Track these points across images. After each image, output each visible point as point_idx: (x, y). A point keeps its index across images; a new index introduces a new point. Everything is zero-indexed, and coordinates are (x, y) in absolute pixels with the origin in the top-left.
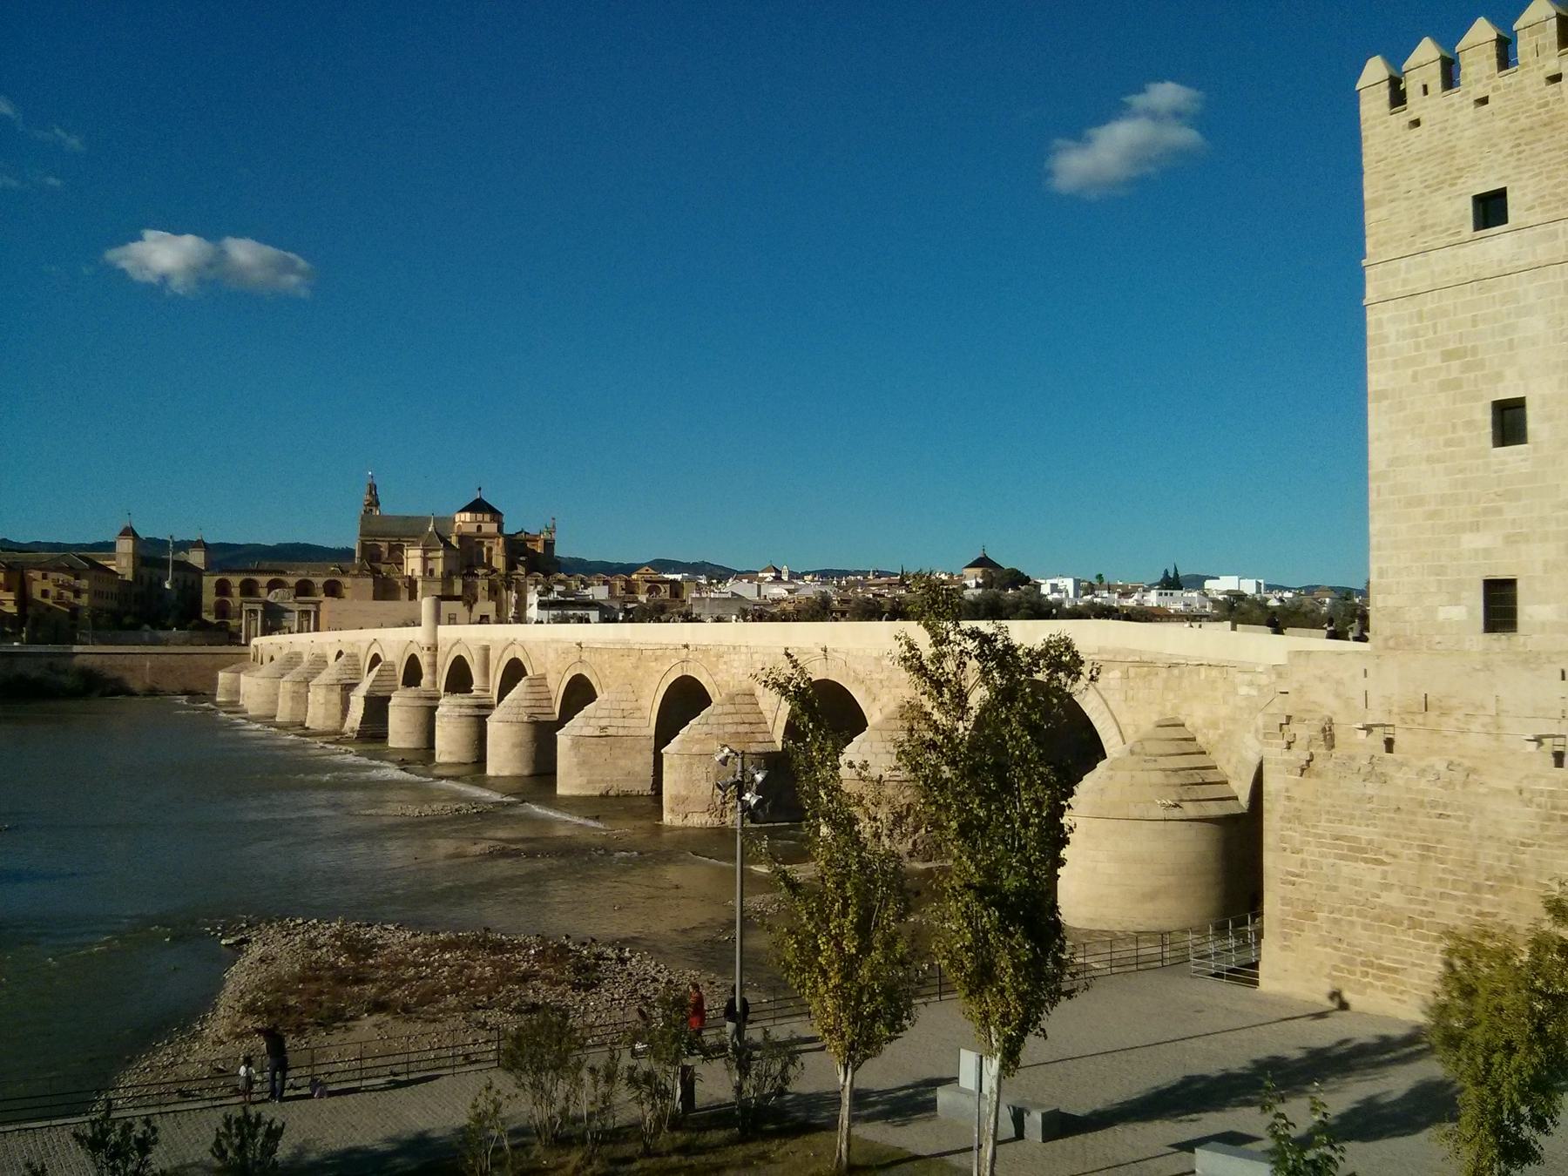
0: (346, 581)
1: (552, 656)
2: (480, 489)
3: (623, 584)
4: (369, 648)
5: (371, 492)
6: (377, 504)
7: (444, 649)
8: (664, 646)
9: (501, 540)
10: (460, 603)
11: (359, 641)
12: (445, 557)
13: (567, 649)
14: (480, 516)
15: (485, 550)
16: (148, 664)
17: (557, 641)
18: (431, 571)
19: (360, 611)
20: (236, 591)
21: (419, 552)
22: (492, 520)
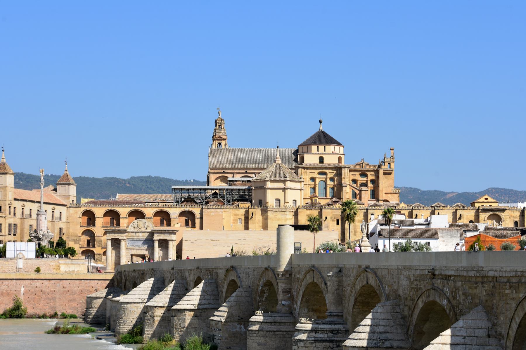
1: (405, 283)
4: (226, 275)
7: (298, 276)
8: (519, 273)
11: (217, 268)
13: (420, 276)
14: (321, 148)
16: (23, 289)
17: (410, 268)
19: (212, 240)
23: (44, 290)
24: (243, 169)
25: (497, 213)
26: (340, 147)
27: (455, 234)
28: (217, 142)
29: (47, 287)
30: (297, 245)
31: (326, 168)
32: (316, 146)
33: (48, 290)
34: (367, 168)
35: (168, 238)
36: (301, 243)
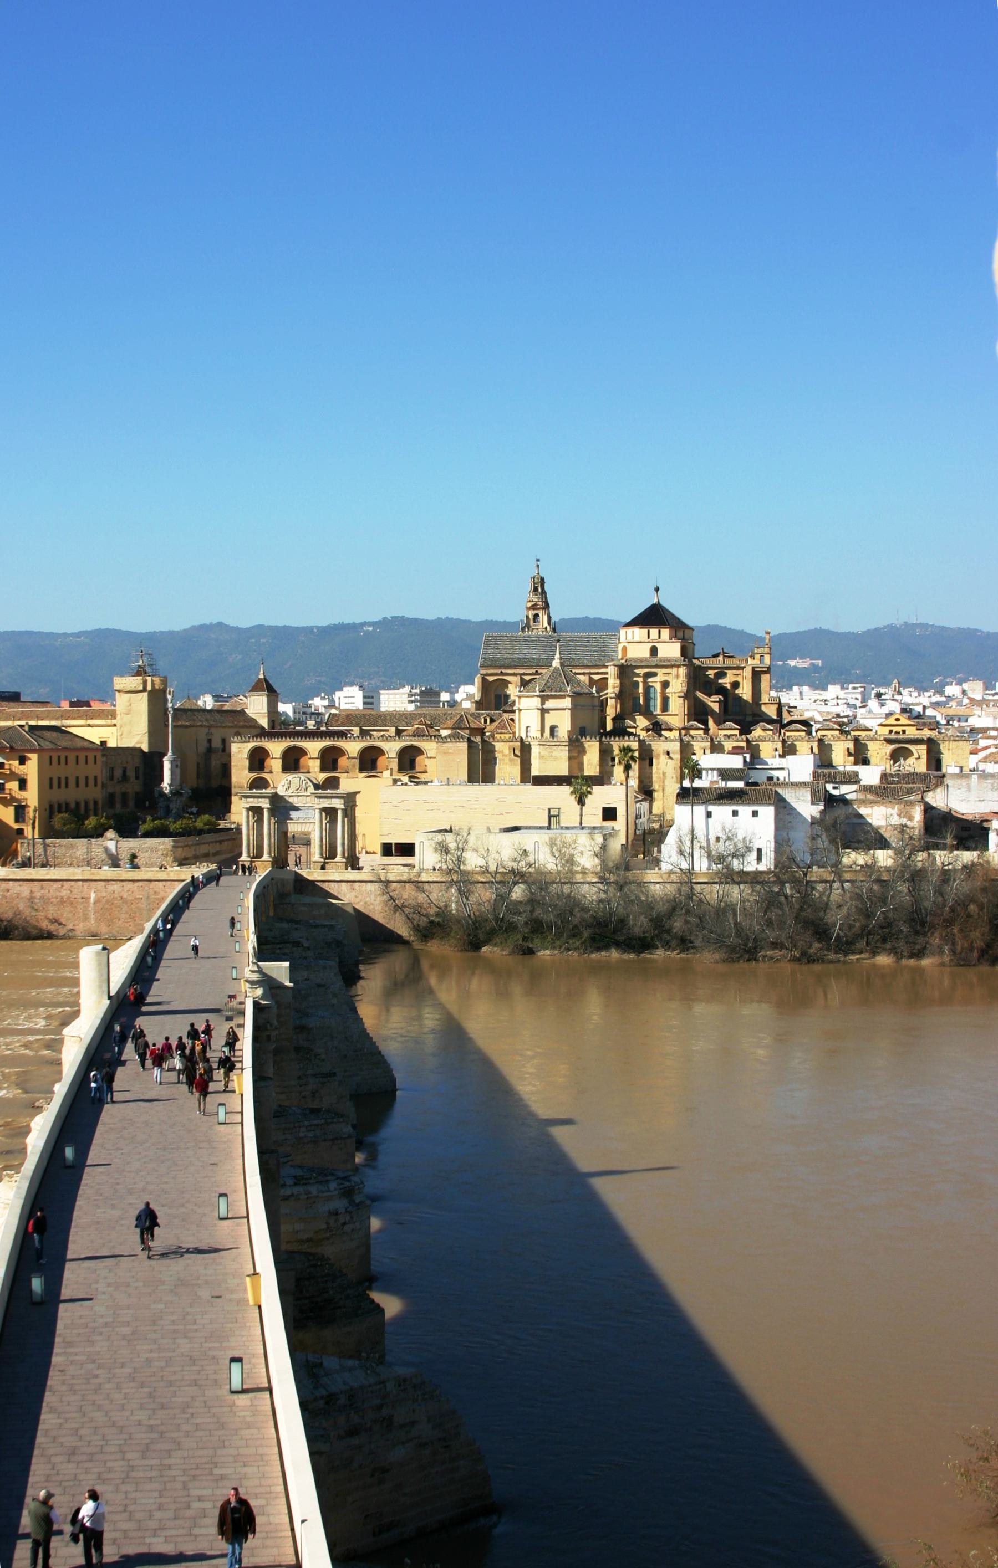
0: (429, 747)
2: (657, 589)
3: (851, 745)
5: (536, 589)
6: (547, 606)
9: (683, 671)
10: (566, 790)
12: (574, 710)
14: (654, 632)
15: (658, 687)
16: (93, 896)
18: (553, 729)
19: (425, 802)
20: (275, 764)
21: (536, 702)
22: (674, 636)
23: (125, 896)
24: (531, 667)
25: (906, 746)
26: (686, 631)
27: (803, 796)
28: (531, 613)
29: (130, 893)
30: (553, 813)
31: (657, 666)
32: (646, 630)
33: (130, 898)
34: (729, 662)
35: (337, 806)
36: (559, 809)
